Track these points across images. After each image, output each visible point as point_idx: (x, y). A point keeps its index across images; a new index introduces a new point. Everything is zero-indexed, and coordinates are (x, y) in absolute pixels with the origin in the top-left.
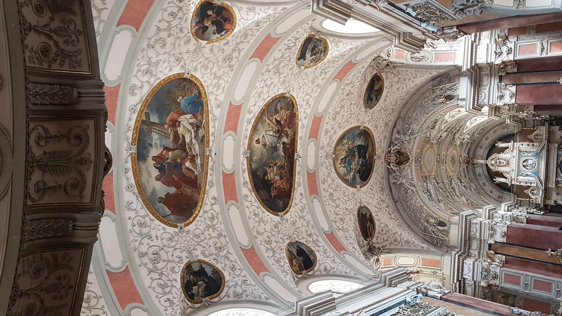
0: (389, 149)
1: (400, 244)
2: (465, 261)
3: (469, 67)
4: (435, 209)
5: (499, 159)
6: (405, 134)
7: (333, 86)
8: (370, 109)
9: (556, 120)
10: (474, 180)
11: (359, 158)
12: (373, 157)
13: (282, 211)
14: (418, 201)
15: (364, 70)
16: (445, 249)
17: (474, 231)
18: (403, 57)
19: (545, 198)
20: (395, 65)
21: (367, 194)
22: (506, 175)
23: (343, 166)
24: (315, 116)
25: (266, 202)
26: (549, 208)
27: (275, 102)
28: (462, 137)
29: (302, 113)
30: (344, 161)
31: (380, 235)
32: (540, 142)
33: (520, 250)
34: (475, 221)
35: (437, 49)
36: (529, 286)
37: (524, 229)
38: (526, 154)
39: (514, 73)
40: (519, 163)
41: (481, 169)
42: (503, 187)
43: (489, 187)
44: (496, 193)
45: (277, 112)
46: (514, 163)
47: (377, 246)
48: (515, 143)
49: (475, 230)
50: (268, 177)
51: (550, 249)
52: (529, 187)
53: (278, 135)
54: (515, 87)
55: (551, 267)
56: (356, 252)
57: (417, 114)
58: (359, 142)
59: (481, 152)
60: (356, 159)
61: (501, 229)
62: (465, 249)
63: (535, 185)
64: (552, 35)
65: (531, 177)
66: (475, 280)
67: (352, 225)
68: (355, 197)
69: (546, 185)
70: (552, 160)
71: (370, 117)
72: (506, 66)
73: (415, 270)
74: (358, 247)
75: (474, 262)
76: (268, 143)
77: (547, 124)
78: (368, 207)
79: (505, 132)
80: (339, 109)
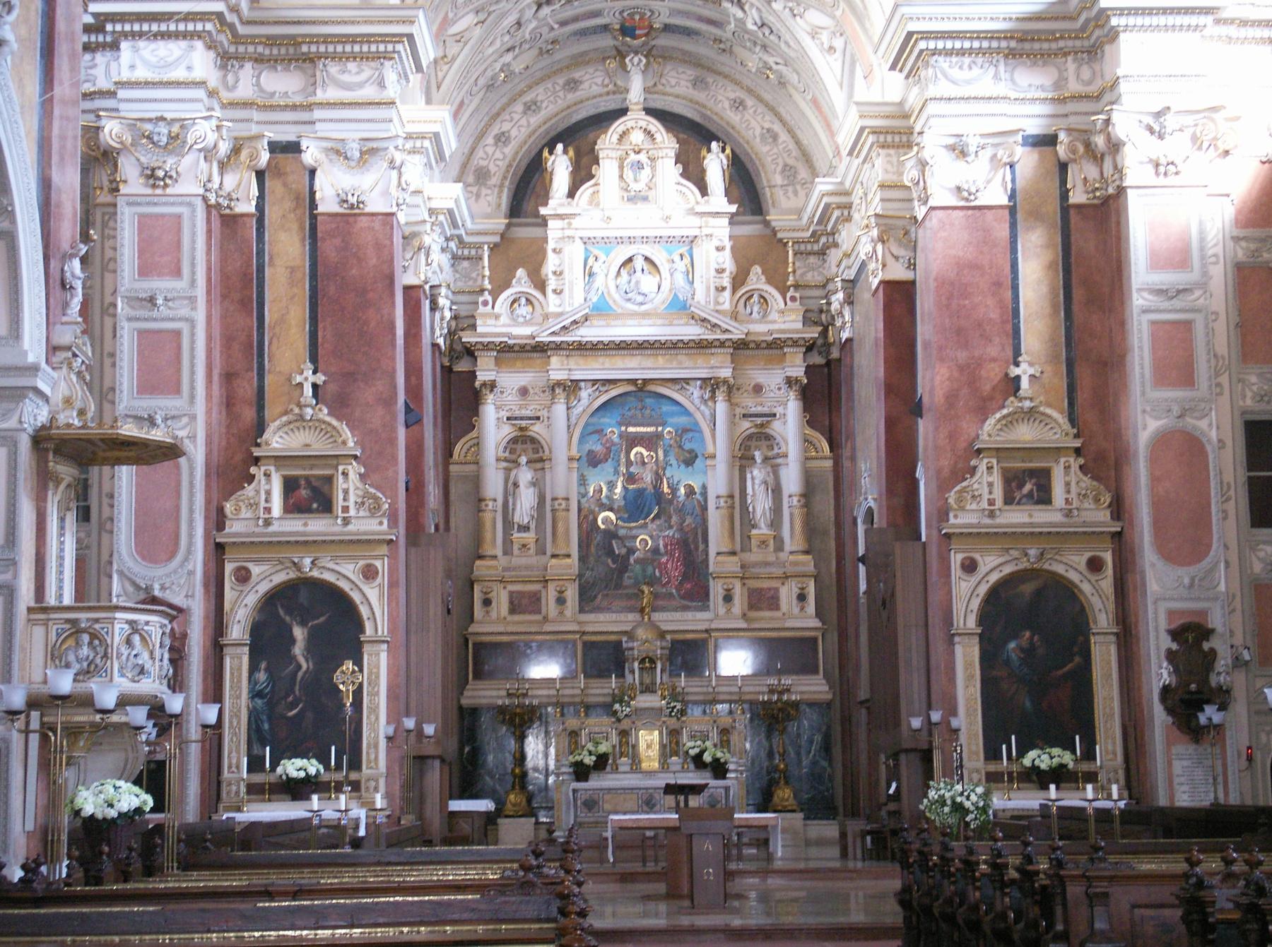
2: (199, 44)
5: (652, 159)
9: (828, 363)
10: (547, 60)
17: (346, 78)
22: (585, 191)
26: (462, 366)
32: (735, 316)
33: (293, 270)
34: (391, 76)
36: (146, 314)
37: (390, 279)
38: (681, 266)
39: (1064, 194)
40: (639, 244)
41: (596, 90)
42: (527, 188)
43: (521, 129)
44: (500, 160)
48: (726, 221)
49: (345, 81)
51: (320, 378)
52: (541, 285)
54: (1004, 201)
55: (246, 388)
59: (679, 89)
61: (372, 189)
62: (252, 40)
63: (552, 308)
64: (1221, 327)
65: (587, 292)
66: (122, 94)
69: (558, 347)
70: (661, 361)
72: (1098, 158)
75: (201, 84)
77: (813, 333)
79: (771, 179)
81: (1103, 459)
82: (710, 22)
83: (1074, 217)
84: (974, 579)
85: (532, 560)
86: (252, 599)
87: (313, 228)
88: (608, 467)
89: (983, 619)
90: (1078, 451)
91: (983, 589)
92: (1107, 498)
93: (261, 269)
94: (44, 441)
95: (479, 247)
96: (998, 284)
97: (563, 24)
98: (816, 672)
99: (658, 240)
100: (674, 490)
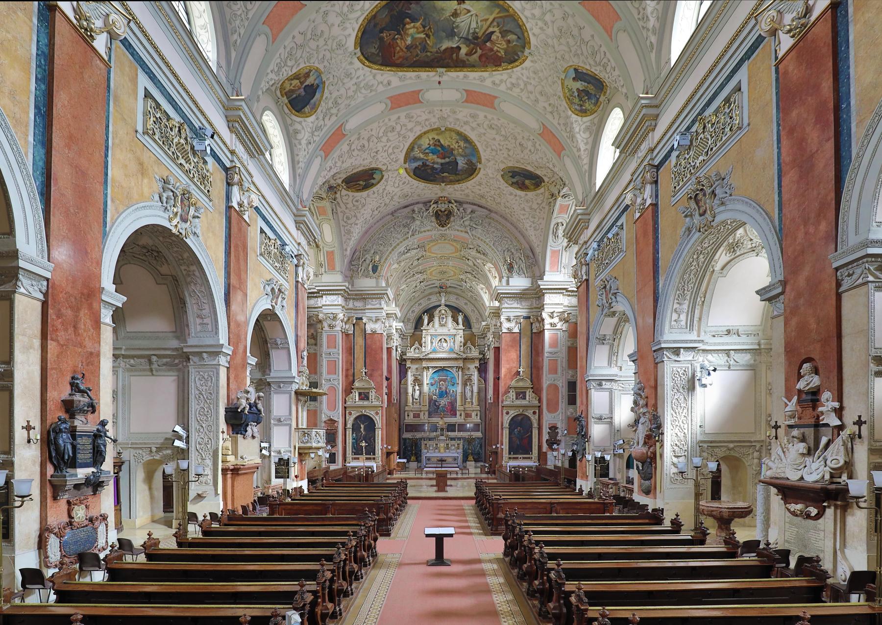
4: (390, 260)
6: (471, 219)
7: (534, 125)
13: (362, 54)
18: (560, 212)
19: (413, 359)
22: (431, 324)
24: (496, 97)
25: (372, 24)
27: (518, 30)
29: (499, 77)
31: (351, 198)
42: (418, 323)
43: (418, 309)
44: (413, 316)
45: (504, 33)
46: (444, 330)
47: (338, 195)
50: (408, 23)
53: (470, 38)
59: (453, 301)
76: (458, 20)
79: (473, 320)
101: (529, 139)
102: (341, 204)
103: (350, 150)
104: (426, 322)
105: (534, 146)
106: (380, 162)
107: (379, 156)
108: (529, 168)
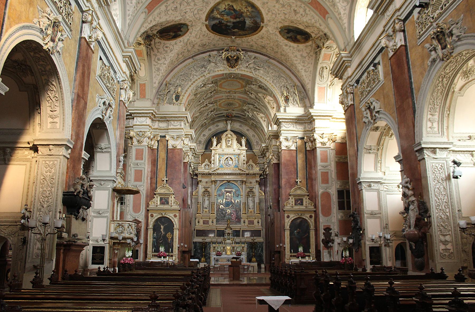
0: (240, 50)
1: (156, 64)
2: (148, 118)
3: (312, 114)
8: (280, 32)
9: (264, 178)
11: (234, 23)
12: (233, 36)
14: (195, 77)
15: (318, 25)
16: (156, 101)
18: (324, 60)
20: (318, 53)
21: (199, 32)
22: (219, 145)
23: (227, 7)
28: (249, 111)
30: (231, 8)
35: (328, 88)
38: (237, 159)
39: (306, 148)
42: (209, 144)
43: (207, 133)
44: (203, 139)
46: (230, 151)
47: (153, 43)
51: (167, 179)
55: (154, 181)
56: (147, 24)
57: (272, 73)
58: (248, 22)
60: (232, 20)
61: (179, 144)
67: (171, 19)
68: (197, 21)
71: (271, 32)
72: (312, 142)
73: (134, 77)
74: (152, 25)
78: (188, 33)
80: (281, 2)
81: (312, 197)
82: (243, 115)
83: (307, 152)
84: (289, 219)
85: (208, 215)
86: (154, 220)
87: (167, 151)
88: (222, 197)
89: (290, 227)
90: (308, 195)
91: (291, 221)
92: (313, 205)
93: (157, 159)
94: (115, 190)
95: (199, 155)
96: (294, 164)
97: (216, 115)
98: (260, 236)
99: (232, 154)
100: (235, 201)
101: (300, 7)
102: (154, 49)
103: (166, 11)
104: (215, 143)
105: (305, 11)
106: (188, 18)
107: (187, 15)
108: (301, 27)
